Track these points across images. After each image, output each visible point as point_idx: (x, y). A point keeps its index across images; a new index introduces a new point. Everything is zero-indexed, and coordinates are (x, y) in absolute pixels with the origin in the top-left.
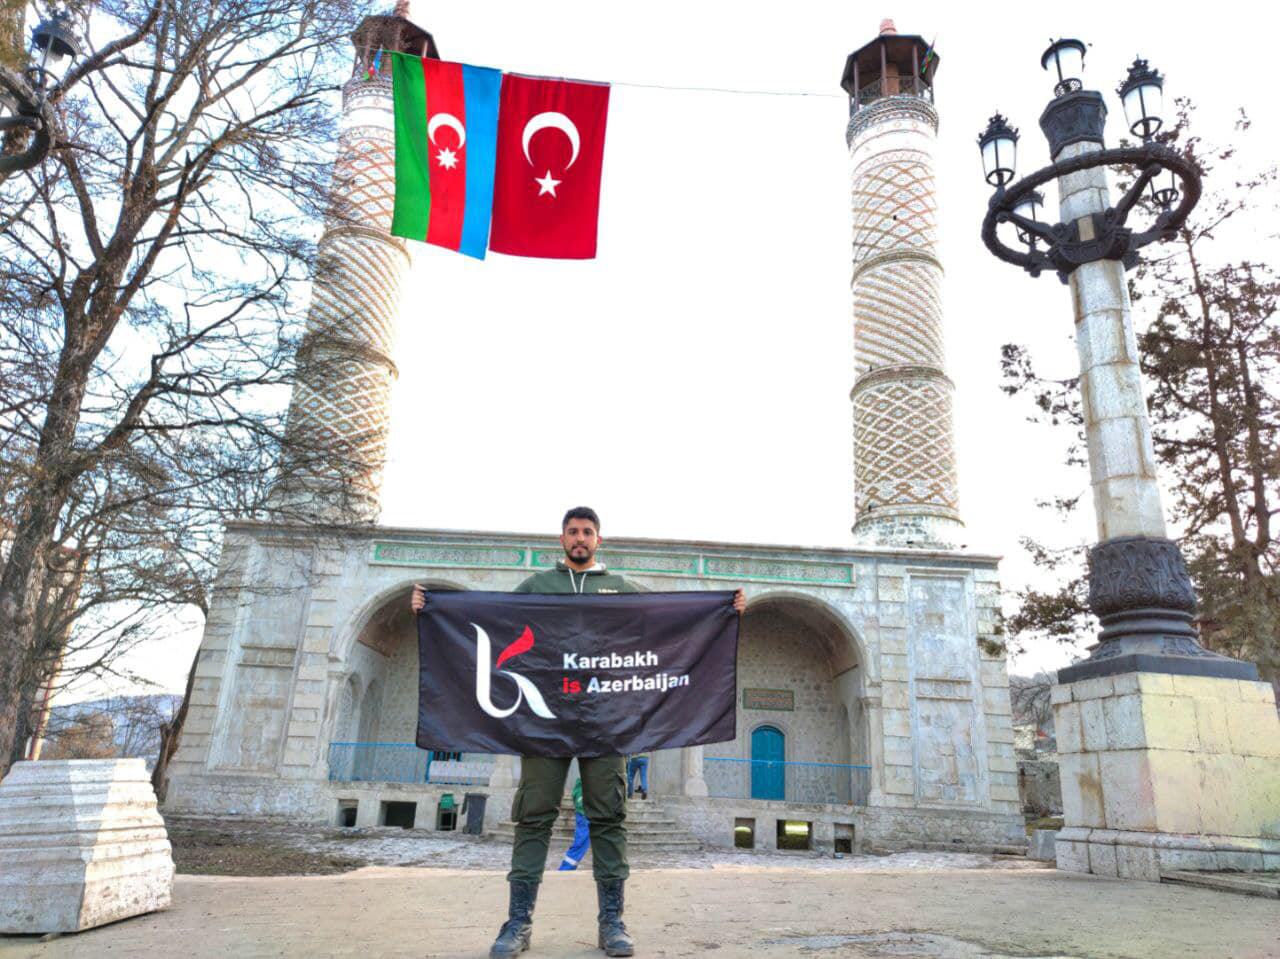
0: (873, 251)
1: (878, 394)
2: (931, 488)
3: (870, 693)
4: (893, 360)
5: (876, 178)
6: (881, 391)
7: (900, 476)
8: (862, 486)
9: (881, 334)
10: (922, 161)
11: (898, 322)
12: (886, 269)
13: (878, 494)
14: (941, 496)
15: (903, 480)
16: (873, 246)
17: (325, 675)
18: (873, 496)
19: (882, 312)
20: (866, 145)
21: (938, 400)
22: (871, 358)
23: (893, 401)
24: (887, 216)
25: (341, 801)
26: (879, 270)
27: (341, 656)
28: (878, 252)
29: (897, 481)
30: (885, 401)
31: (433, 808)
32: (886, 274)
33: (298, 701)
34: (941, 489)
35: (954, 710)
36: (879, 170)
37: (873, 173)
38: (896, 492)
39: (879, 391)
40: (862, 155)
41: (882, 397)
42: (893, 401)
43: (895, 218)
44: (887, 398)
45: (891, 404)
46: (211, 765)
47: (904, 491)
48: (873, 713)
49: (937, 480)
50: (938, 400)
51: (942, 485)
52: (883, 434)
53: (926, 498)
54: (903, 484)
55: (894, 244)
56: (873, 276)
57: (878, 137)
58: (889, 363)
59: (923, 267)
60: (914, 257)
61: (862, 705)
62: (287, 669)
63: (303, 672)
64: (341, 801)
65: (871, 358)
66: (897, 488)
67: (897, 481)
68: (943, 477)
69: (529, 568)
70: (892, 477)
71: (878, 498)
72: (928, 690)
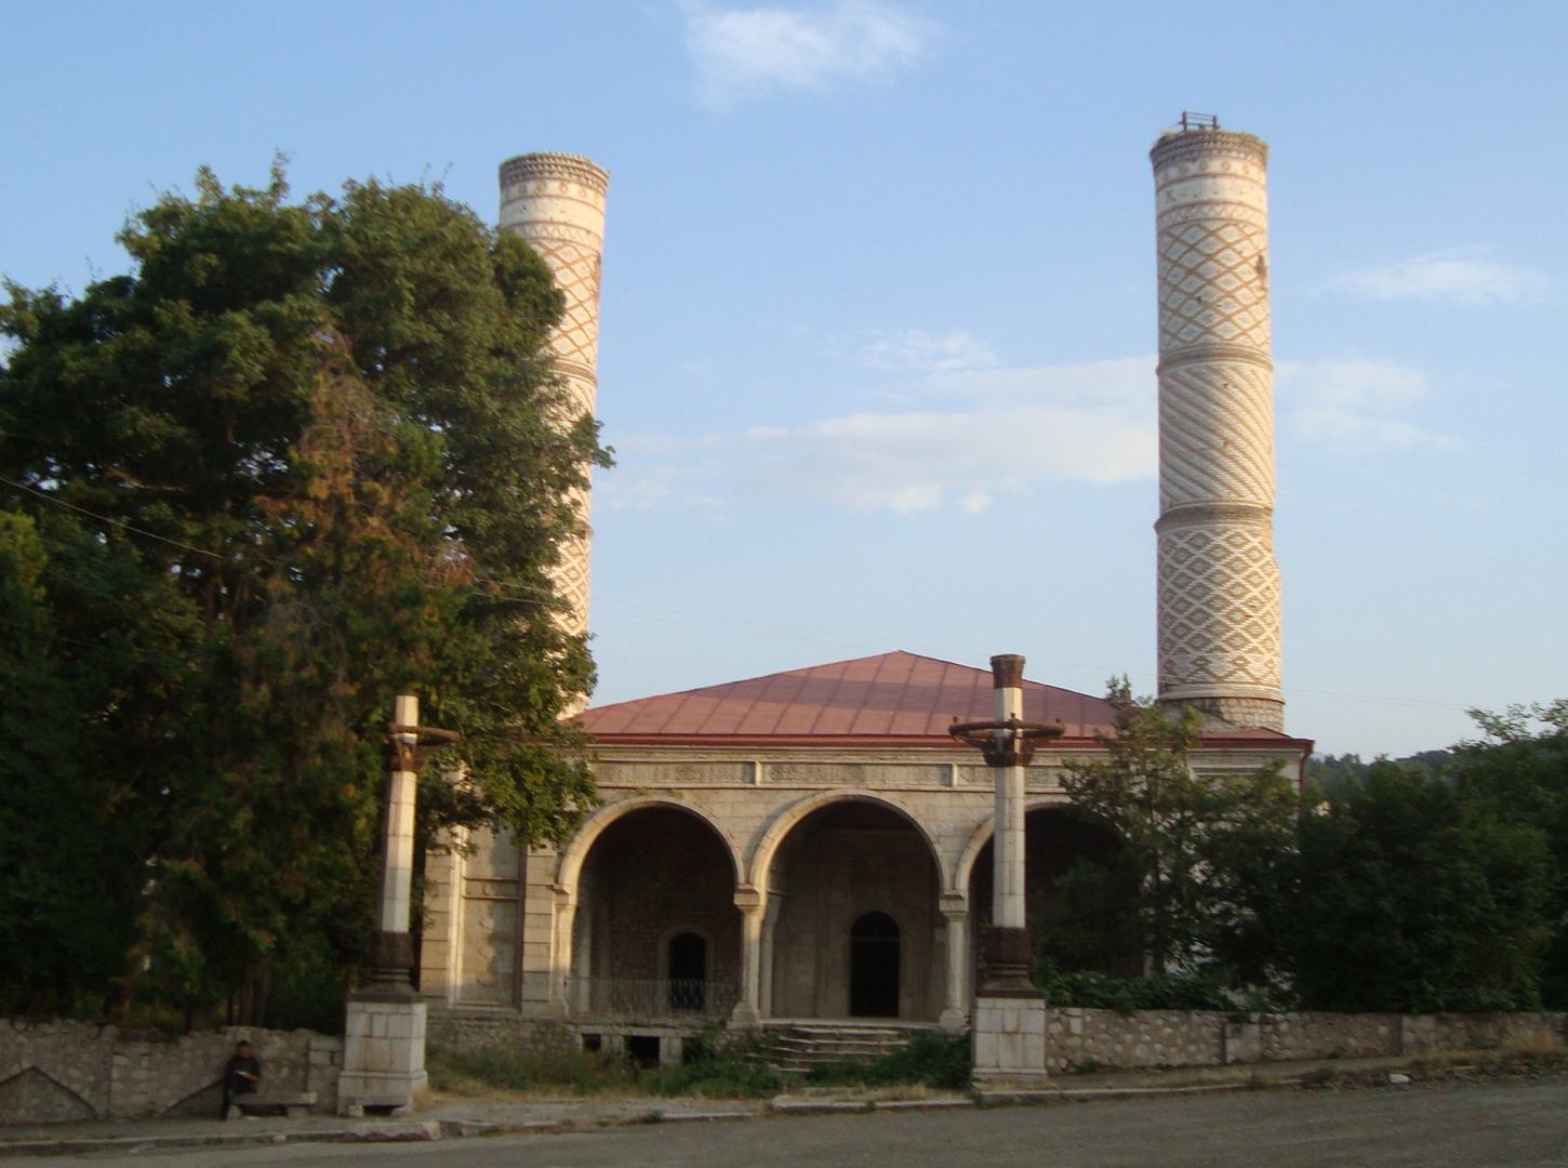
0: (1175, 343)
1: (1175, 539)
2: (1234, 662)
4: (1193, 496)
5: (1177, 239)
6: (1181, 538)
7: (1198, 649)
9: (1182, 458)
10: (1235, 216)
11: (1202, 445)
12: (1188, 371)
13: (1175, 670)
14: (1245, 670)
15: (1201, 654)
16: (1174, 336)
19: (1182, 429)
20: (1168, 189)
21: (1247, 547)
22: (1175, 491)
23: (1192, 550)
24: (1191, 296)
25: (584, 1035)
26: (1181, 371)
28: (1181, 345)
30: (1182, 549)
31: (677, 1045)
33: (528, 935)
34: (1248, 662)
36: (1182, 229)
37: (1176, 232)
38: (1194, 668)
39: (1177, 535)
41: (1181, 544)
42: (1192, 550)
43: (1199, 299)
44: (1186, 546)
45: (1190, 555)
46: (451, 1000)
47: (1202, 668)
49: (1241, 653)
50: (1247, 547)
51: (1248, 657)
52: (1181, 593)
53: (1227, 676)
55: (1199, 337)
56: (1174, 377)
57: (1180, 181)
58: (1190, 499)
59: (1233, 369)
63: (531, 905)
64: (584, 1035)
65: (1175, 491)
66: (1194, 663)
67: (1194, 654)
68: (1250, 646)
69: (758, 785)
70: (1189, 649)
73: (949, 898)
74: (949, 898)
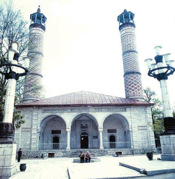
3: (130, 130)
6: (129, 76)
8: (126, 93)
17: (36, 133)
18: (129, 95)
26: (127, 54)
27: (39, 129)
29: (133, 92)
32: (128, 55)
35: (144, 131)
38: (133, 94)
40: (122, 33)
48: (131, 133)
54: (134, 92)
60: (133, 73)
61: (129, 131)
62: (31, 132)
63: (33, 132)
71: (130, 95)
72: (140, 128)
73: (100, 128)
74: (100, 128)
